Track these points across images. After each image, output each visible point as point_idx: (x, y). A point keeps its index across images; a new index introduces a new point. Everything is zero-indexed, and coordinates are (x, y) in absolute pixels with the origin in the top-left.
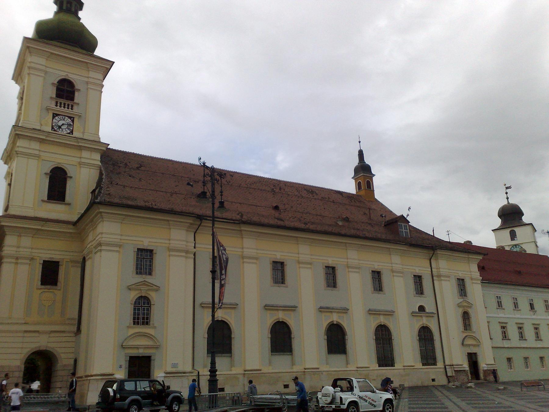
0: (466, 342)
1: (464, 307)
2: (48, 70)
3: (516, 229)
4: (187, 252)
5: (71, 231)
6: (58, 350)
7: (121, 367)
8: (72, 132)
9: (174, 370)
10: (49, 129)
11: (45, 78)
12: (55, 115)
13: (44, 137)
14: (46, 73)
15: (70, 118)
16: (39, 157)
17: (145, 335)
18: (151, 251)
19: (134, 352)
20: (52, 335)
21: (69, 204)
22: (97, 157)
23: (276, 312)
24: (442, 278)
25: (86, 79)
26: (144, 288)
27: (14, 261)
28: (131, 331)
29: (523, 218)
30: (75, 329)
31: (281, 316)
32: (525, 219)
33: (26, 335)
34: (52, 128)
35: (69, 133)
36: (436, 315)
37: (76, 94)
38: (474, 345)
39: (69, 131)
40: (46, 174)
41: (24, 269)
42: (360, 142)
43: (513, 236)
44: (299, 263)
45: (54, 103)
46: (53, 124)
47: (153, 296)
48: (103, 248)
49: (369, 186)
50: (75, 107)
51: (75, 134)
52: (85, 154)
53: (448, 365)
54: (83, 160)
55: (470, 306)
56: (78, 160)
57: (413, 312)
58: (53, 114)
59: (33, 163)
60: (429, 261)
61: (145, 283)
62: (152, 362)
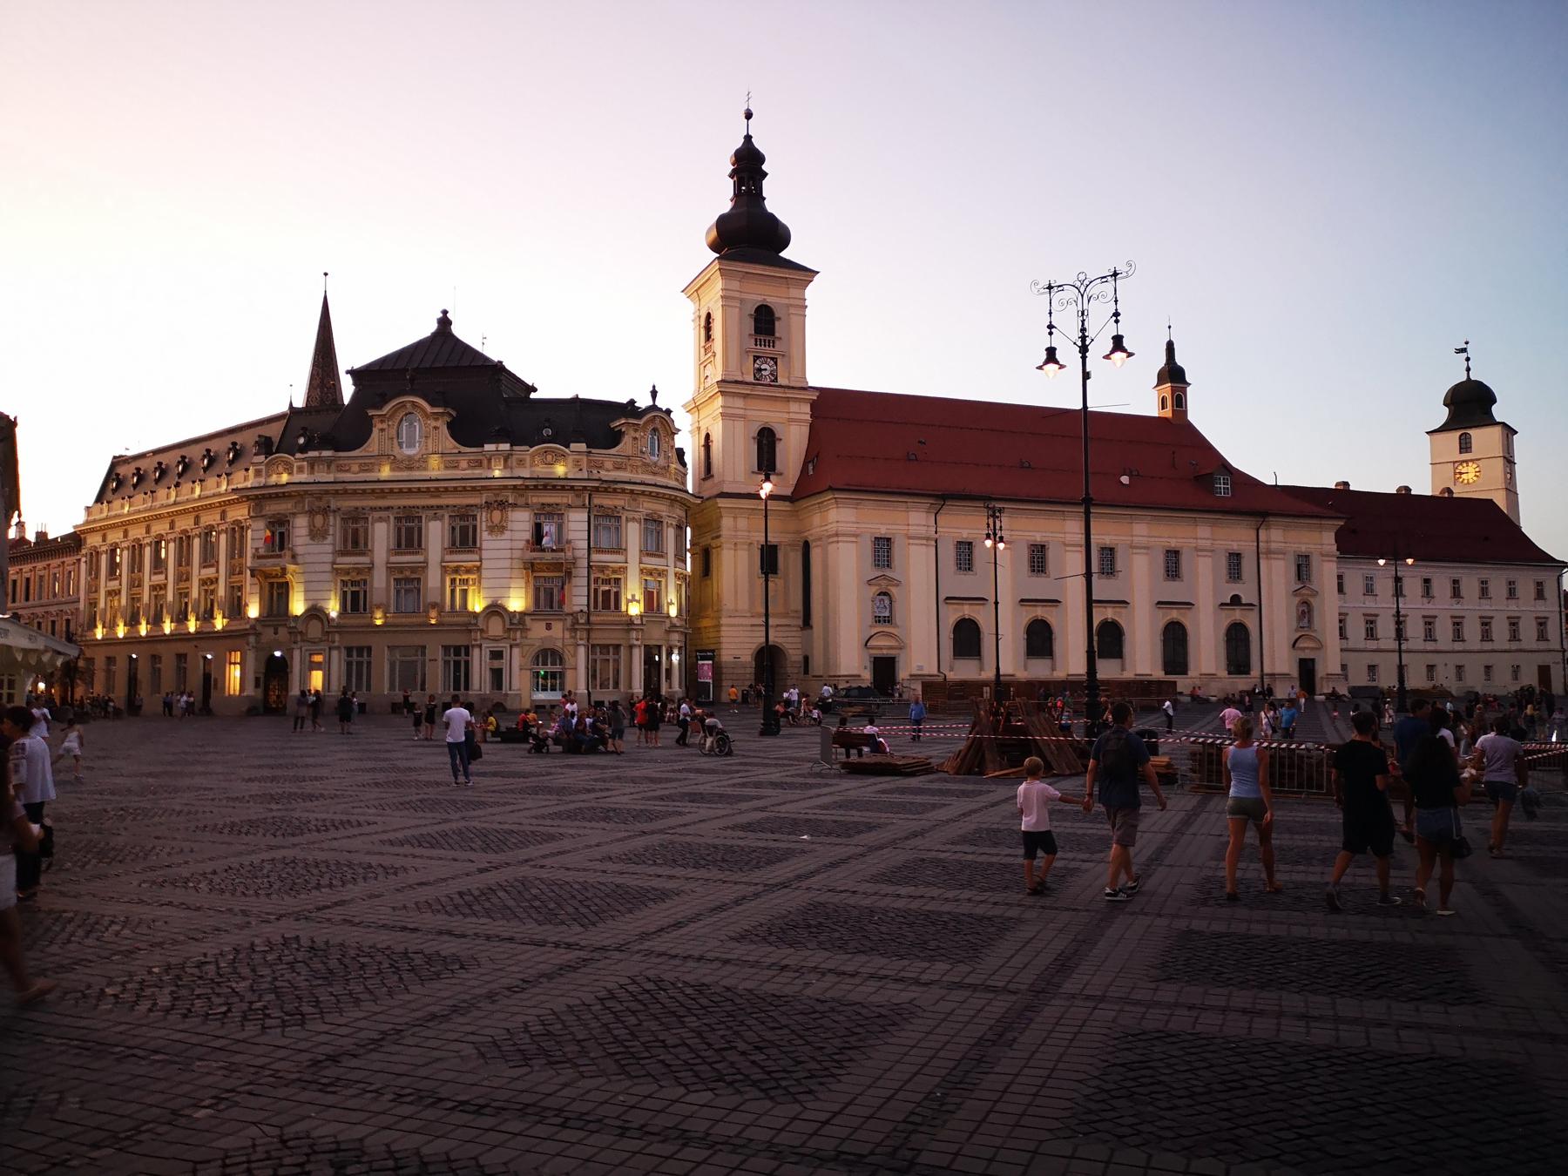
0: (1300, 644)
1: (1304, 595)
2: (744, 296)
3: (1473, 433)
4: (928, 539)
5: (788, 509)
6: (787, 646)
7: (866, 668)
8: (776, 379)
9: (920, 673)
10: (750, 379)
11: (740, 309)
12: (756, 358)
14: (742, 301)
15: (772, 359)
16: (743, 417)
17: (890, 635)
18: (889, 540)
19: (877, 653)
20: (779, 629)
21: (781, 474)
22: (807, 408)
23: (1034, 608)
24: (1273, 556)
25: (786, 301)
26: (884, 583)
28: (874, 631)
29: (1494, 408)
30: (800, 622)
31: (1039, 612)
32: (1498, 412)
36: (1257, 609)
37: (777, 323)
38: (1312, 649)
40: (754, 438)
41: (743, 555)
42: (1170, 327)
43: (1465, 446)
44: (1065, 545)
45: (753, 341)
47: (894, 590)
48: (840, 539)
49: (1179, 401)
50: (777, 343)
51: (781, 381)
52: (794, 407)
53: (1267, 675)
55: (1315, 594)
56: (787, 416)
57: (1222, 604)
59: (740, 425)
60: (1254, 533)
62: (897, 664)
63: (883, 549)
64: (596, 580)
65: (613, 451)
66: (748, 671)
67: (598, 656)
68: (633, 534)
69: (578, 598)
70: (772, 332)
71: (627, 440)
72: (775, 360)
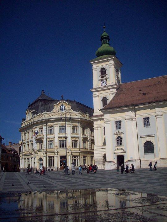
10: (100, 86)
25: (108, 65)
27: (97, 129)
28: (117, 148)
33: (102, 149)
47: (122, 136)
52: (111, 90)
54: (111, 93)
61: (119, 132)
63: (118, 124)
64: (49, 141)
65: (51, 112)
66: (101, 160)
67: (50, 159)
68: (56, 130)
69: (44, 146)
71: (55, 108)
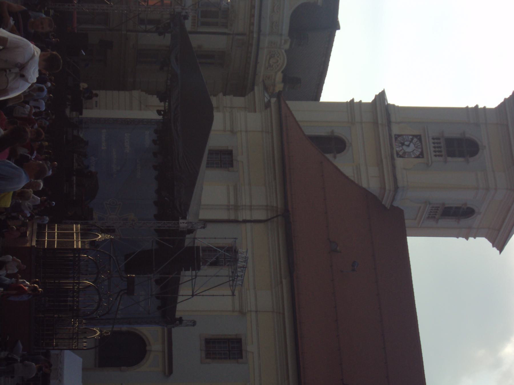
8: (401, 157)
13: (380, 122)
34: (399, 136)
35: (398, 154)
39: (401, 153)
40: (332, 132)
46: (404, 137)
51: (399, 162)
58: (420, 136)
70: (451, 154)
72: (421, 155)
